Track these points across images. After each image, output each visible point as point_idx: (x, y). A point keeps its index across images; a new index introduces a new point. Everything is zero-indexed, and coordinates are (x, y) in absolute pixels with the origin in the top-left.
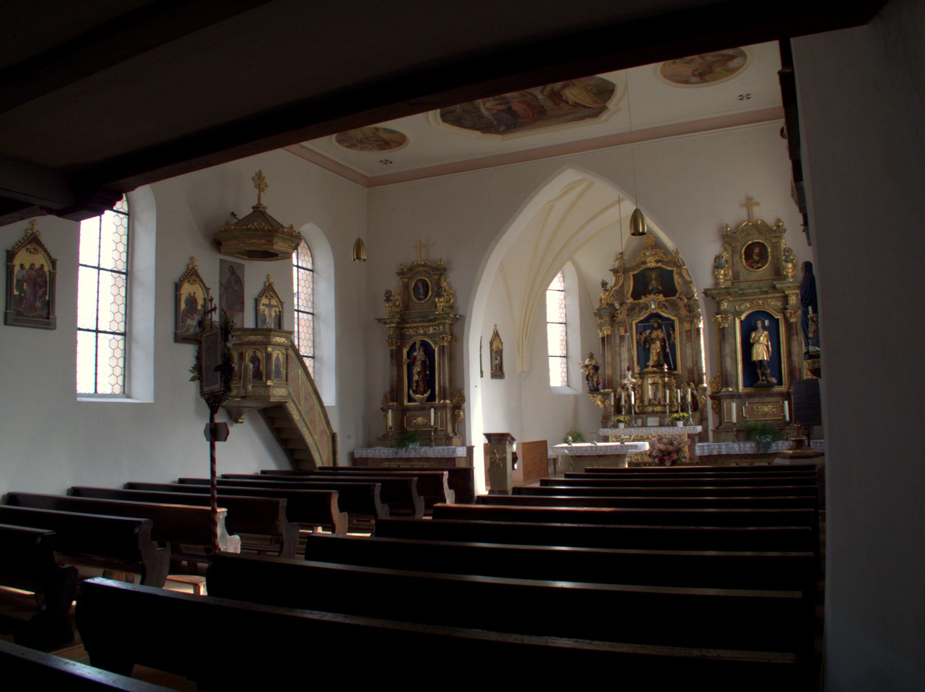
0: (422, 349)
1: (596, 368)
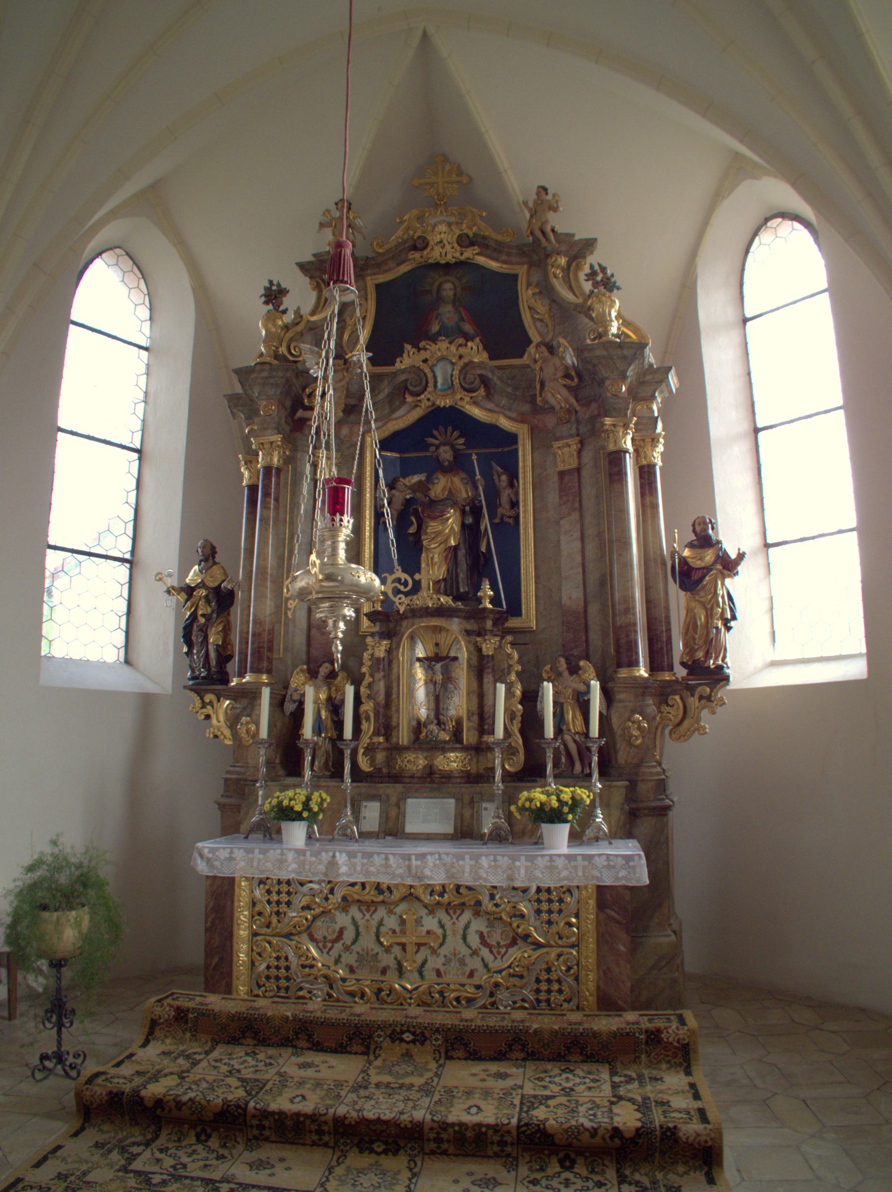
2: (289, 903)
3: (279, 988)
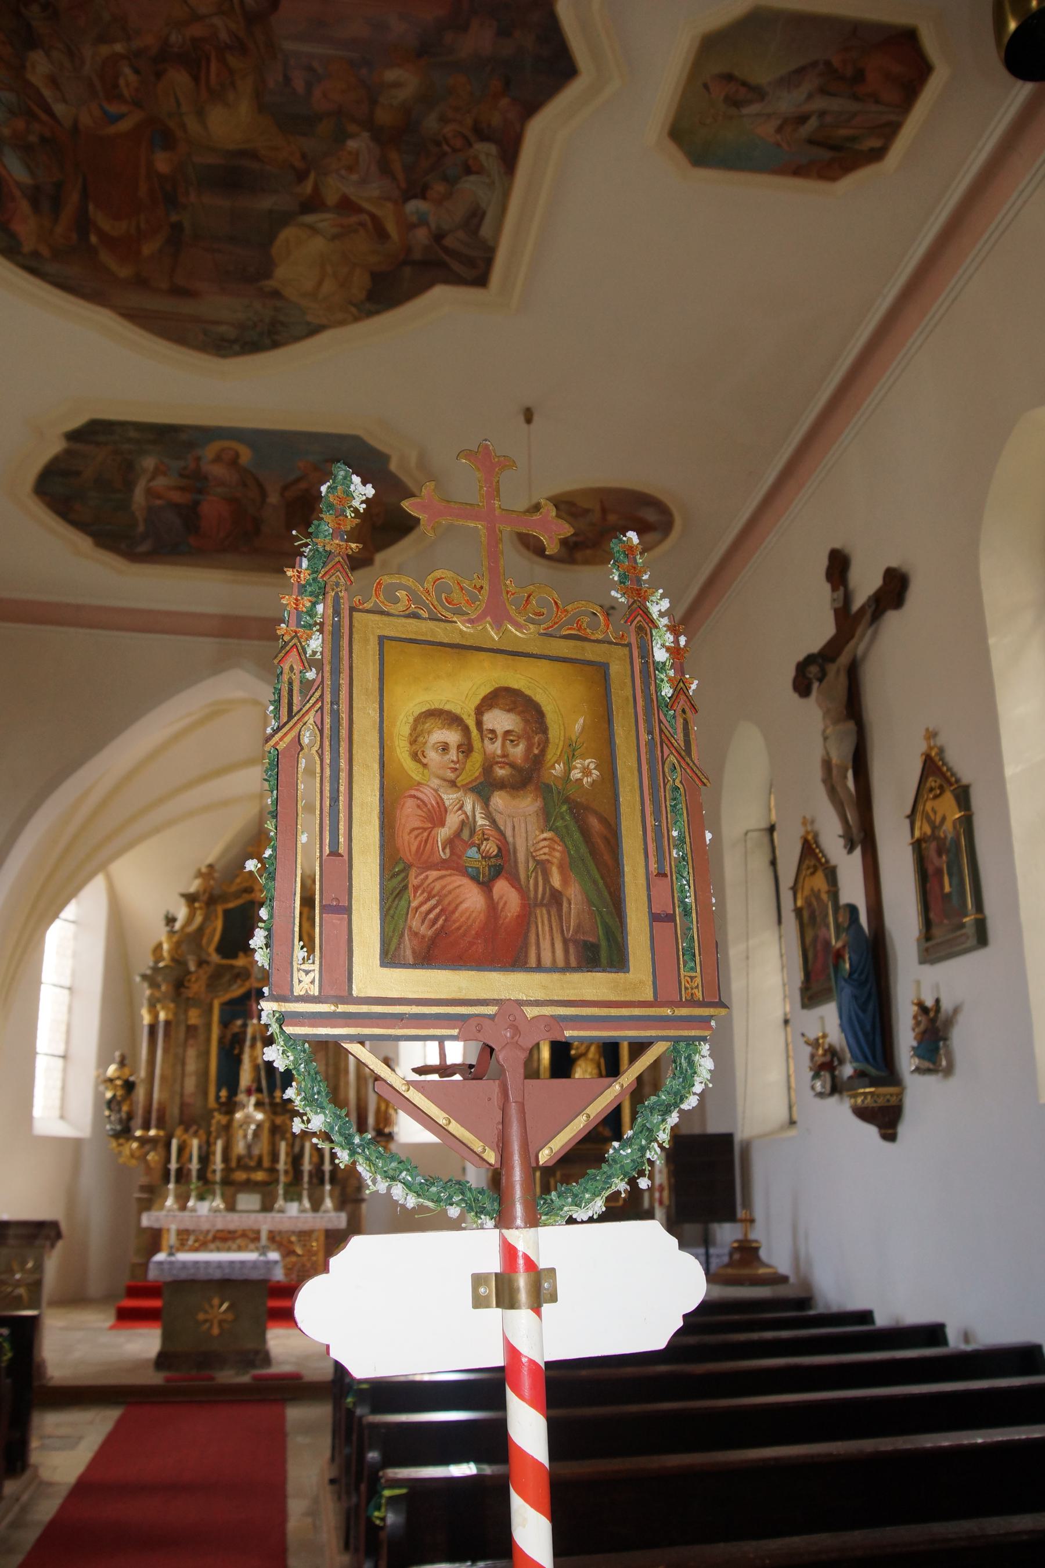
1: (129, 1086)
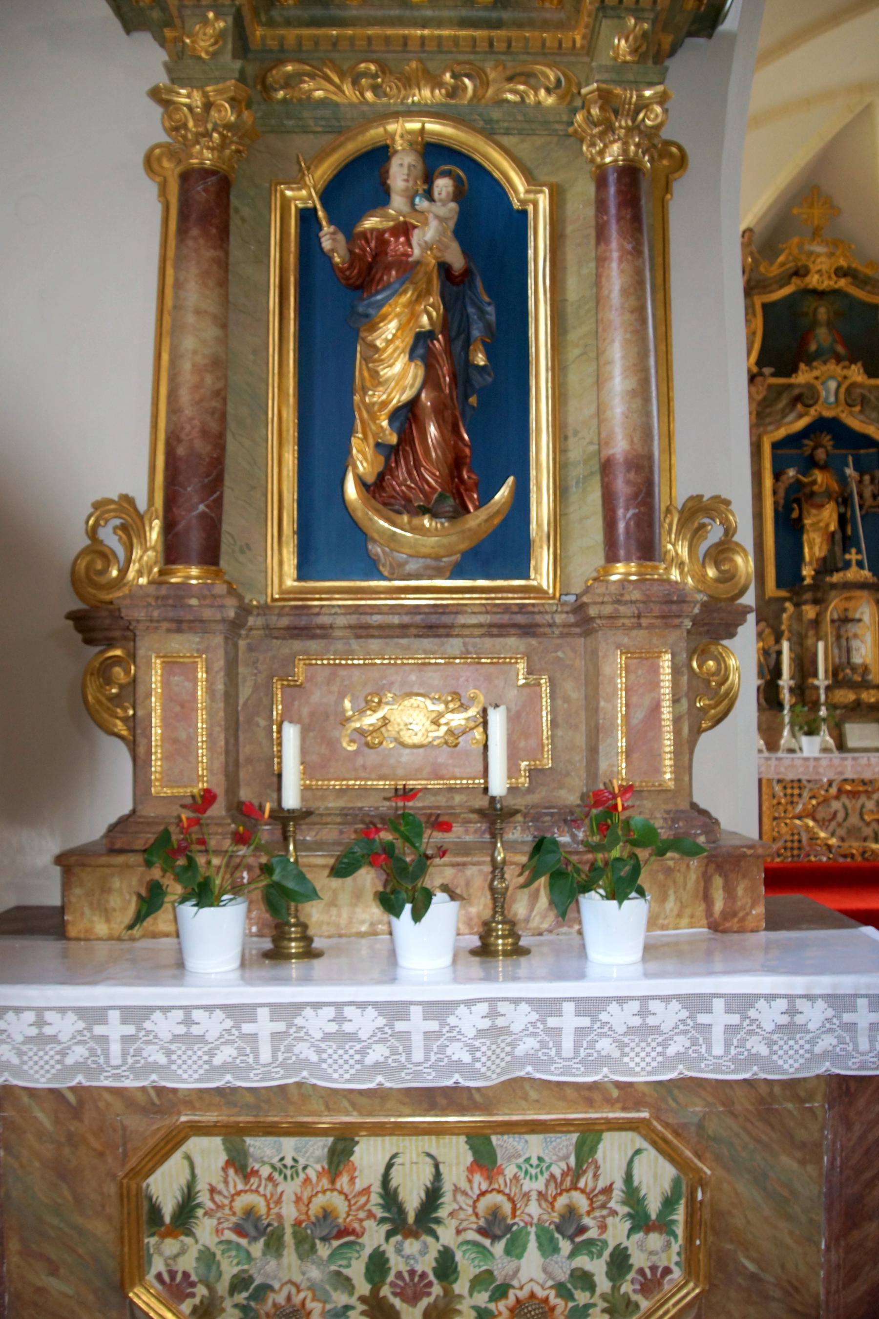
0: (443, 185)
2: (800, 795)
3: (793, 856)
